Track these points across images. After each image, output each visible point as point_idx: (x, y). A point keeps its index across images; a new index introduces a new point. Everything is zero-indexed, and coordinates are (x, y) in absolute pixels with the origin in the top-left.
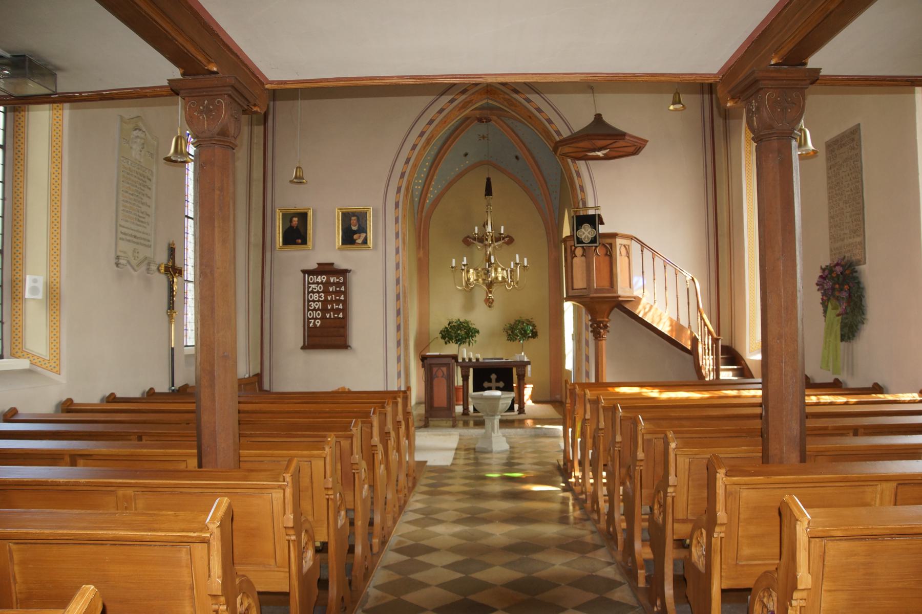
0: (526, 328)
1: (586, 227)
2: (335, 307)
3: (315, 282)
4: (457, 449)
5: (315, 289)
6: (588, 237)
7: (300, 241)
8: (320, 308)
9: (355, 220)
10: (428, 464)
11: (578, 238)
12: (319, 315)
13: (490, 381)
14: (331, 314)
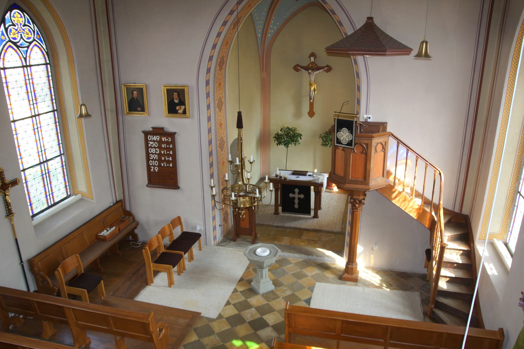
1: (345, 131)
2: (167, 159)
3: (152, 140)
4: (241, 280)
5: (153, 145)
6: (345, 139)
7: (140, 109)
8: (157, 159)
9: (176, 95)
10: (202, 315)
11: (337, 139)
12: (156, 163)
13: (294, 193)
14: (164, 164)
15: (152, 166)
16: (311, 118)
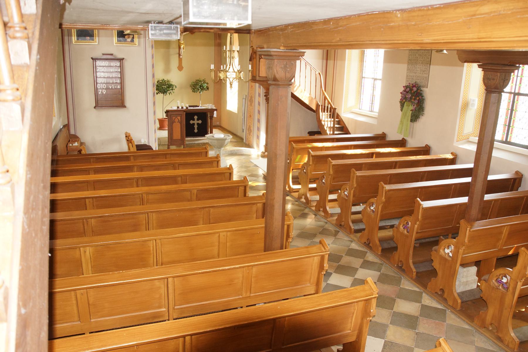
0: (204, 85)
12: (104, 87)
13: (194, 120)
15: (101, 89)
16: (180, 71)
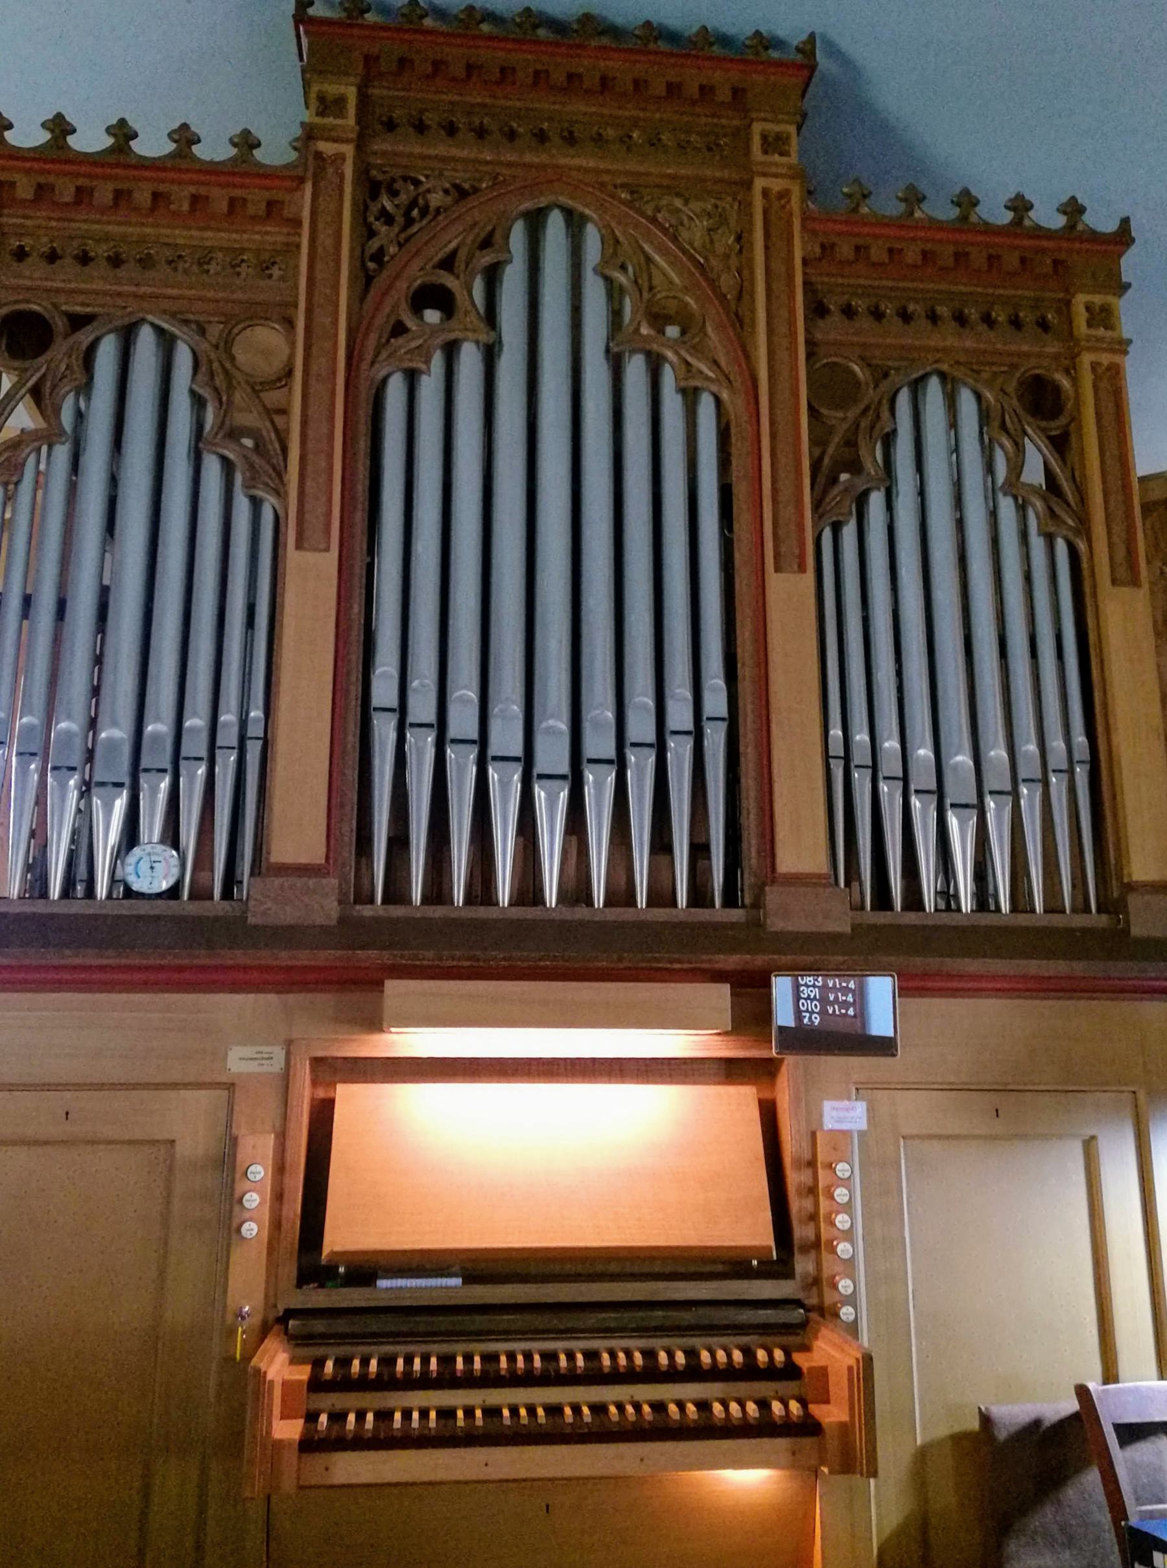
2: (841, 998)
15: (807, 1011)
